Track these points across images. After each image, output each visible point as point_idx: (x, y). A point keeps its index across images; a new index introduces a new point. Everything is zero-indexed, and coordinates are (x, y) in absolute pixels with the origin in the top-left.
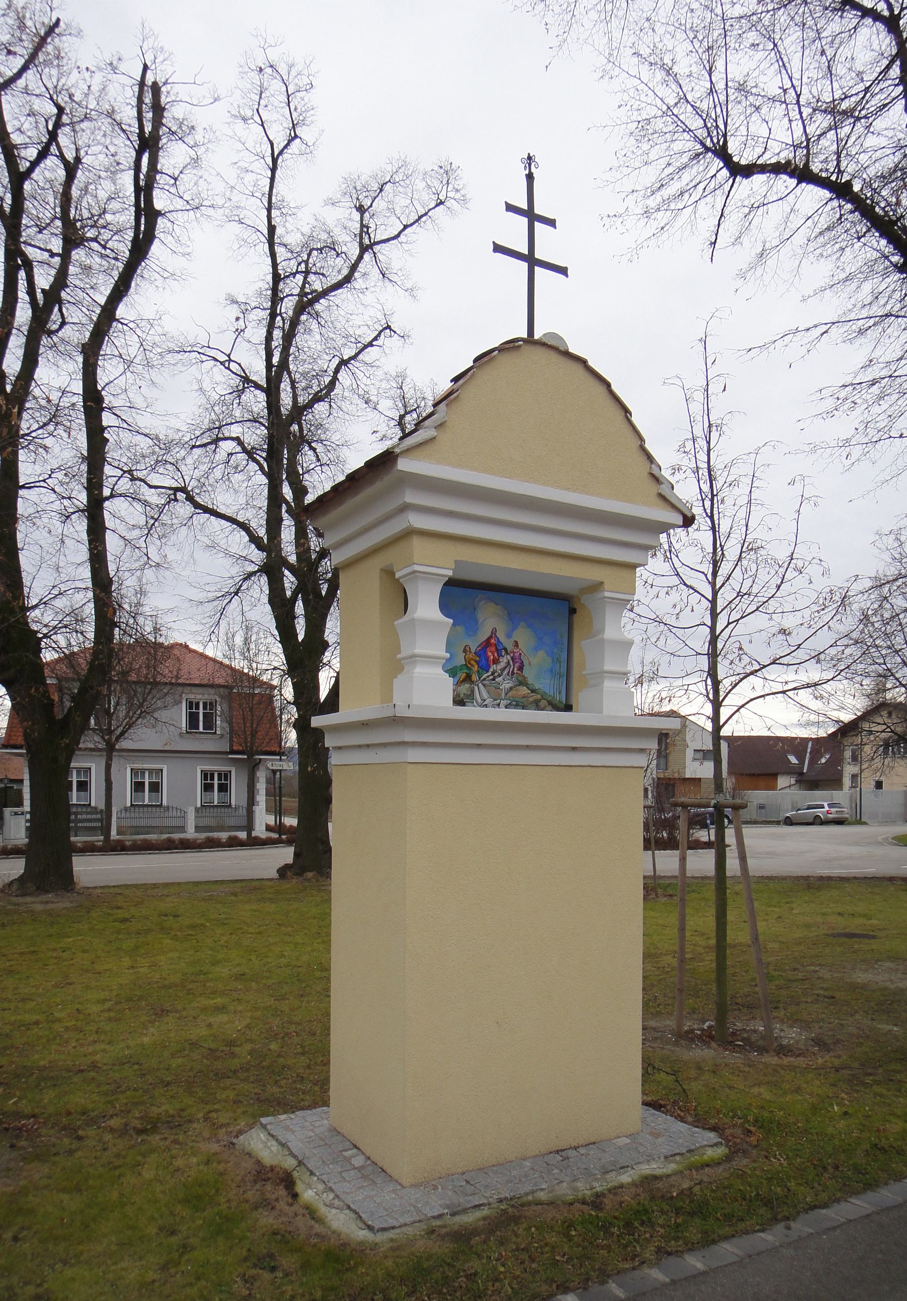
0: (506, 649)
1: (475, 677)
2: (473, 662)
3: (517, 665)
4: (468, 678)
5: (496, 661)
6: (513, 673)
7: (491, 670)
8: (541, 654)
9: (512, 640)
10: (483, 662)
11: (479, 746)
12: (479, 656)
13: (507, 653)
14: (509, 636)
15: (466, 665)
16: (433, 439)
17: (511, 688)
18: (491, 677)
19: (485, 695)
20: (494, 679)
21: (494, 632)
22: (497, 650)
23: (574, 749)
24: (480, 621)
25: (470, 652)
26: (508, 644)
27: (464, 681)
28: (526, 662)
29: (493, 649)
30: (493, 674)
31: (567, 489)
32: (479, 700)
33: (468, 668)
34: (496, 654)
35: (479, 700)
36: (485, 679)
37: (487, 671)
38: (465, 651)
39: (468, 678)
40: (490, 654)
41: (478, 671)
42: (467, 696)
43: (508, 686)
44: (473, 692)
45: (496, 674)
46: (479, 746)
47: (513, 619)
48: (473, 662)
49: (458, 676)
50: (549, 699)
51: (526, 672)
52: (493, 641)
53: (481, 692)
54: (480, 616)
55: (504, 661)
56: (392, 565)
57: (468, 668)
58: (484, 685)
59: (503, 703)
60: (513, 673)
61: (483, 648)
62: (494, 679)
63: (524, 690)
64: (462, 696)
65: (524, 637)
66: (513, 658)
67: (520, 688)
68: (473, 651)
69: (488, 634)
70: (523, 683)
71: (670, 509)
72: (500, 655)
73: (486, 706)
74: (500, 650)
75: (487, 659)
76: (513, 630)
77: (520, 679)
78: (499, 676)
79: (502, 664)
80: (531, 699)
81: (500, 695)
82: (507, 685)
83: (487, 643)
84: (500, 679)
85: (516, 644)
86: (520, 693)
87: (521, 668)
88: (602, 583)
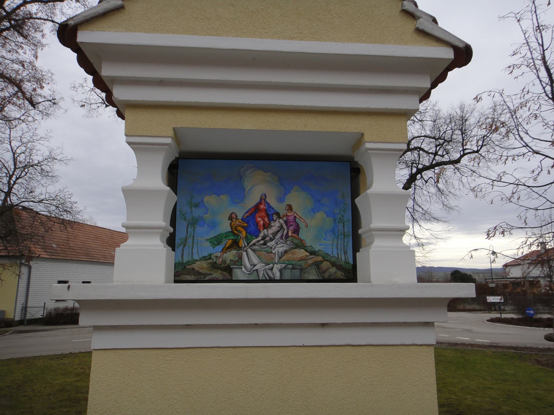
0: (278, 214)
1: (242, 243)
2: (239, 228)
3: (291, 228)
4: (235, 245)
5: (267, 226)
6: (287, 236)
7: (262, 234)
8: (320, 215)
9: (285, 204)
10: (252, 228)
12: (248, 223)
14: (280, 200)
15: (232, 232)
17: (286, 252)
18: (262, 242)
19: (255, 260)
20: (265, 244)
21: (263, 198)
22: (268, 215)
25: (237, 219)
26: (281, 208)
27: (230, 247)
28: (302, 225)
29: (263, 214)
30: (263, 238)
31: (292, 38)
34: (266, 219)
36: (254, 244)
37: (257, 236)
38: (231, 218)
39: (235, 245)
40: (259, 219)
41: (246, 237)
42: (235, 263)
43: (281, 250)
44: (241, 257)
45: (267, 239)
47: (285, 184)
48: (239, 228)
49: (224, 243)
50: (333, 260)
51: (303, 234)
52: (262, 206)
54: (247, 184)
55: (275, 226)
58: (254, 251)
60: (287, 236)
61: (251, 214)
62: (265, 244)
63: (301, 253)
64: (228, 262)
65: (298, 201)
66: (286, 222)
67: (297, 250)
68: (240, 217)
69: (258, 200)
70: (300, 245)
72: (271, 219)
74: (271, 215)
75: (257, 224)
76: (285, 194)
77: (296, 241)
78: (271, 240)
79: (274, 229)
80: (310, 262)
81: (273, 259)
82: (280, 249)
83: (256, 209)
84: (273, 243)
85: (290, 208)
86: (296, 256)
87: (297, 231)
88: (363, 134)
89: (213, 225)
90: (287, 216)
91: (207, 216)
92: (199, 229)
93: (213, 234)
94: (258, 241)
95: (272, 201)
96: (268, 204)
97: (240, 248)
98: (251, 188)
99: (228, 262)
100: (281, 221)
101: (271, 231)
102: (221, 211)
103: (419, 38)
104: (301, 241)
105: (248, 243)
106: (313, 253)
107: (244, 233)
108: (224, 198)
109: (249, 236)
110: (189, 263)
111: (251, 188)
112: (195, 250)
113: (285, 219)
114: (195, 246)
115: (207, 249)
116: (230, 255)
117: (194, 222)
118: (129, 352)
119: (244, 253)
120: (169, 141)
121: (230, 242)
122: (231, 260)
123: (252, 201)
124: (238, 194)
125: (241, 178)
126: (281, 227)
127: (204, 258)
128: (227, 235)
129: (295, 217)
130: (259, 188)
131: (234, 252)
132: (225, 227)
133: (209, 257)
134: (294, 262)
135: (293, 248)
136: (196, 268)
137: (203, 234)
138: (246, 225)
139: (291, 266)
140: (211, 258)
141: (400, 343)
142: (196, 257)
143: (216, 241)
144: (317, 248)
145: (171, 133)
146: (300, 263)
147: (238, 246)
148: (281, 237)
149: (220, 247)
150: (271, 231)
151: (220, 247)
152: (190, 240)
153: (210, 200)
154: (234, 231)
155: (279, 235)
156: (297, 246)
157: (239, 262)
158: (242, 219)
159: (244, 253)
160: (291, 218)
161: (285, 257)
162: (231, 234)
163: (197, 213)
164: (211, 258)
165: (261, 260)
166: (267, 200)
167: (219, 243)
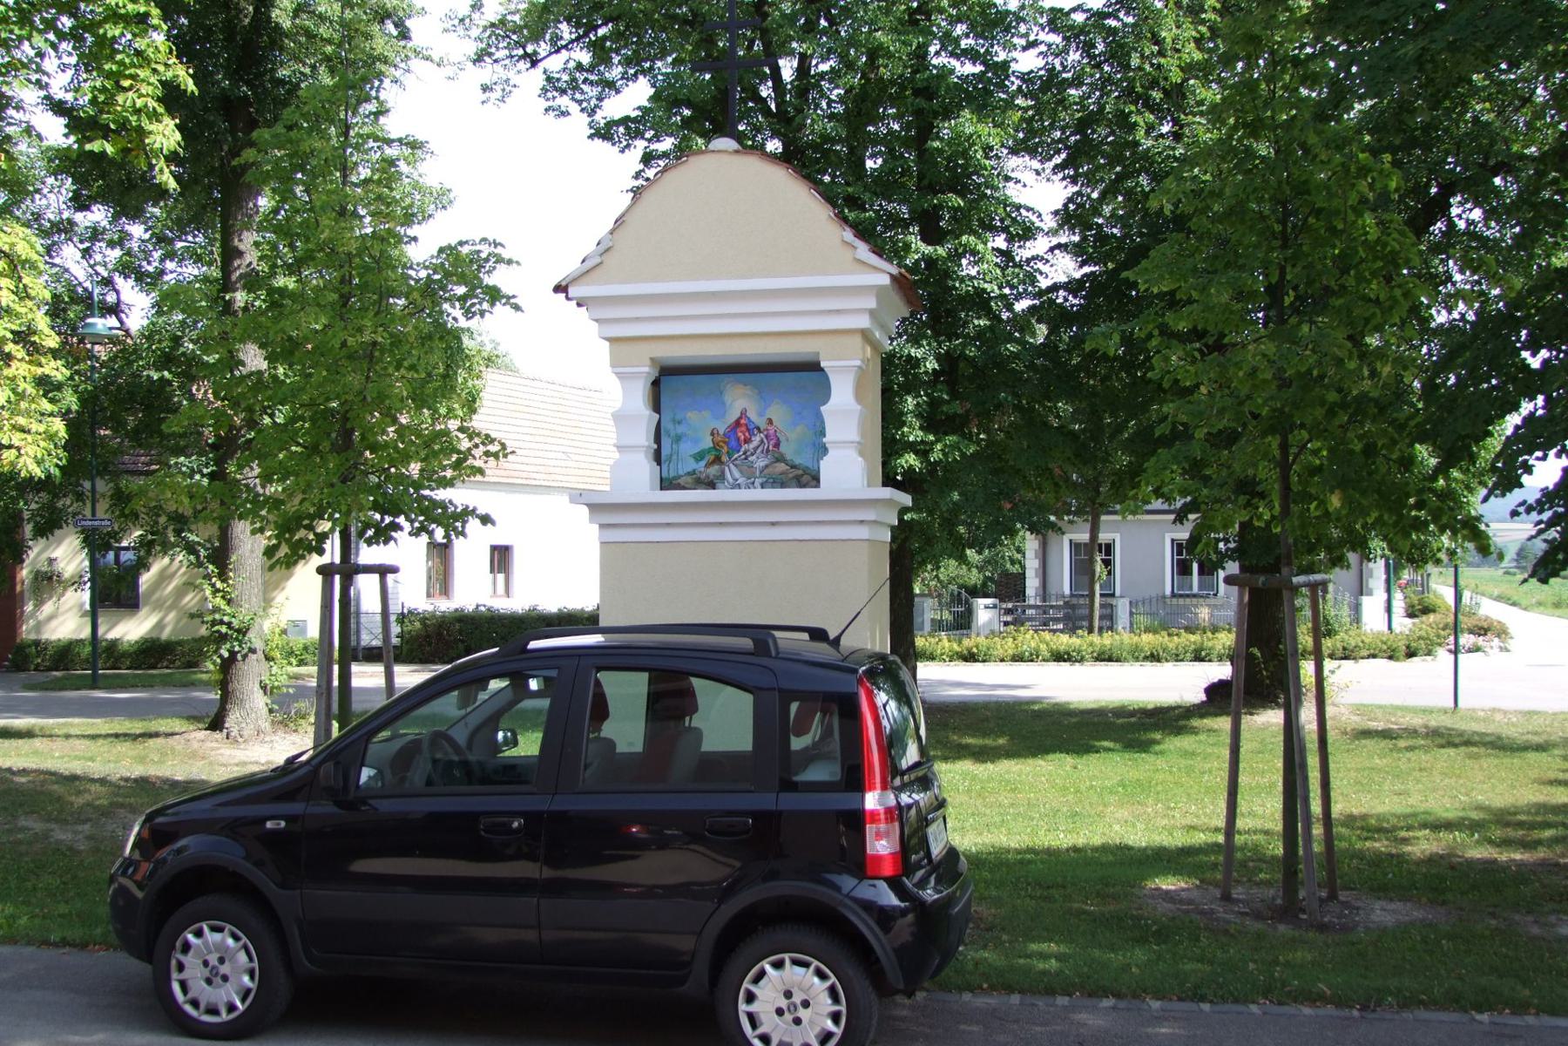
1: (725, 458)
4: (718, 460)
5: (747, 441)
8: (799, 429)
10: (733, 443)
14: (761, 415)
19: (737, 474)
21: (743, 414)
23: (773, 524)
26: (762, 424)
27: (713, 463)
39: (718, 460)
44: (723, 472)
51: (783, 448)
53: (732, 472)
54: (728, 398)
55: (756, 440)
59: (758, 481)
63: (782, 467)
65: (778, 413)
70: (780, 459)
73: (739, 486)
74: (752, 430)
82: (761, 463)
83: (737, 423)
85: (770, 422)
87: (777, 445)
89: (696, 441)
95: (752, 415)
101: (752, 446)
102: (701, 425)
106: (793, 467)
108: (707, 414)
115: (692, 465)
116: (713, 470)
117: (678, 439)
120: (647, 369)
123: (733, 415)
127: (689, 474)
128: (709, 451)
132: (707, 443)
133: (694, 472)
137: (688, 449)
143: (699, 457)
144: (797, 461)
149: (703, 463)
150: (752, 446)
151: (703, 463)
153: (692, 416)
154: (716, 446)
156: (778, 460)
157: (722, 477)
163: (680, 429)
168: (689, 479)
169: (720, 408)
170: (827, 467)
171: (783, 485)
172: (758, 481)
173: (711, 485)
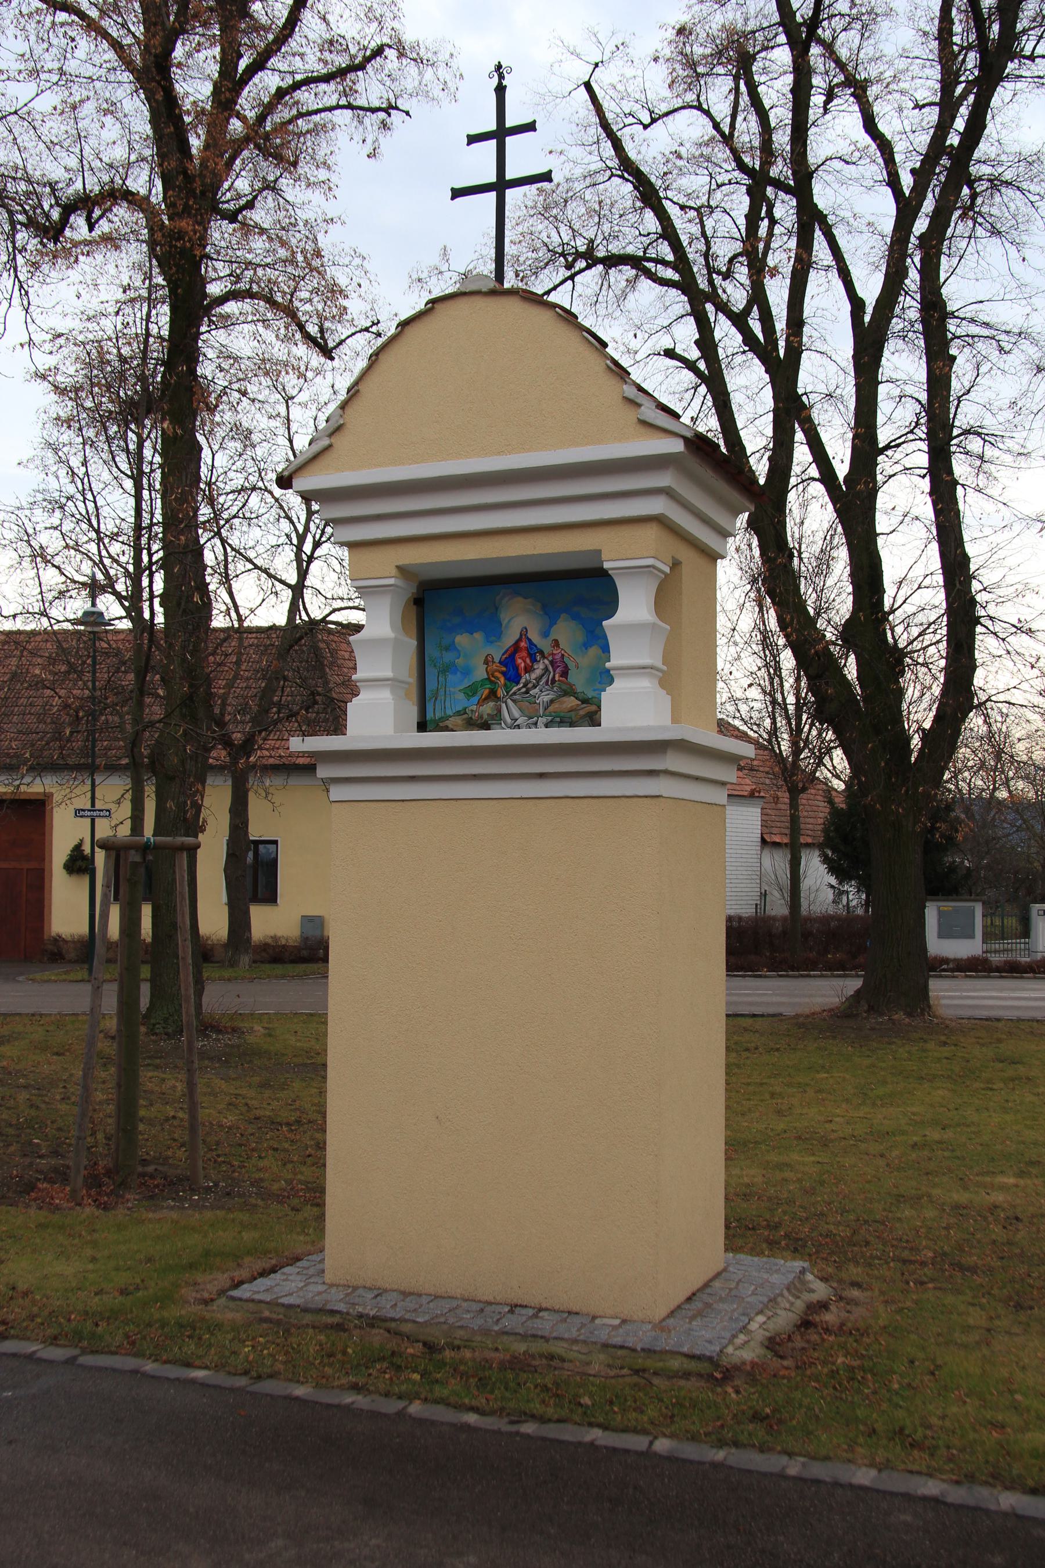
0: (542, 653)
1: (501, 693)
2: (497, 674)
3: (558, 670)
4: (493, 695)
5: (529, 670)
6: (553, 681)
7: (523, 680)
10: (512, 672)
11: (542, 776)
12: (506, 666)
13: (544, 657)
14: (545, 634)
15: (488, 679)
16: (330, 446)
17: (552, 701)
18: (524, 690)
19: (516, 713)
20: (527, 692)
21: (524, 633)
24: (504, 623)
25: (493, 662)
26: (544, 645)
28: (571, 665)
29: (524, 654)
30: (525, 685)
32: (509, 720)
33: (492, 682)
34: (528, 661)
35: (509, 720)
36: (515, 693)
37: (518, 683)
38: (486, 662)
39: (493, 695)
40: (519, 661)
41: (505, 685)
43: (546, 699)
44: (499, 711)
45: (530, 685)
46: (542, 776)
47: (550, 613)
48: (497, 674)
49: (479, 694)
51: (574, 677)
52: (523, 644)
53: (510, 710)
54: (504, 616)
55: (539, 668)
56: (598, 552)
57: (492, 682)
59: (542, 721)
60: (553, 681)
61: (510, 656)
62: (527, 692)
63: (571, 702)
64: (485, 717)
66: (552, 663)
67: (565, 699)
68: (497, 660)
69: (518, 636)
71: (662, 435)
72: (534, 660)
73: (519, 727)
74: (534, 653)
75: (516, 668)
76: (551, 626)
77: (564, 687)
78: (535, 687)
79: (538, 672)
80: (582, 713)
81: (538, 710)
84: (537, 690)
86: (564, 706)
87: (565, 674)
89: (467, 672)
90: (553, 654)
91: (459, 662)
92: (450, 677)
93: (466, 683)
94: (519, 689)
95: (534, 636)
96: (530, 640)
97: (499, 699)
98: (509, 621)
99: (485, 717)
100: (546, 661)
101: (534, 676)
102: (475, 653)
103: (642, 430)
104: (571, 685)
105: (508, 693)
107: (502, 679)
108: (478, 636)
109: (508, 683)
110: (442, 719)
111: (509, 621)
112: (448, 704)
113: (550, 658)
114: (448, 699)
116: (488, 708)
117: (447, 669)
118: (362, 804)
119: (504, 705)
121: (486, 692)
122: (488, 715)
123: (509, 639)
124: (493, 630)
125: (497, 609)
126: (546, 669)
127: (458, 713)
129: (563, 655)
130: (519, 621)
131: (491, 704)
134: (562, 714)
135: (560, 696)
136: (450, 726)
137: (457, 685)
138: (504, 669)
139: (558, 719)
140: (465, 713)
141: (620, 794)
142: (449, 712)
143: (471, 691)
145: (394, 571)
146: (568, 715)
147: (496, 697)
148: (547, 683)
150: (534, 676)
152: (442, 692)
153: (462, 640)
154: (490, 679)
155: (544, 680)
156: (566, 693)
158: (500, 662)
159: (504, 705)
160: (558, 657)
161: (551, 708)
162: (487, 682)
163: (448, 657)
164: (465, 713)
165: (523, 714)
166: (529, 635)
167: (474, 694)
168: (459, 720)
169: (493, 630)
170: (610, 699)
171: (572, 725)
172: (542, 721)
173: (486, 726)
